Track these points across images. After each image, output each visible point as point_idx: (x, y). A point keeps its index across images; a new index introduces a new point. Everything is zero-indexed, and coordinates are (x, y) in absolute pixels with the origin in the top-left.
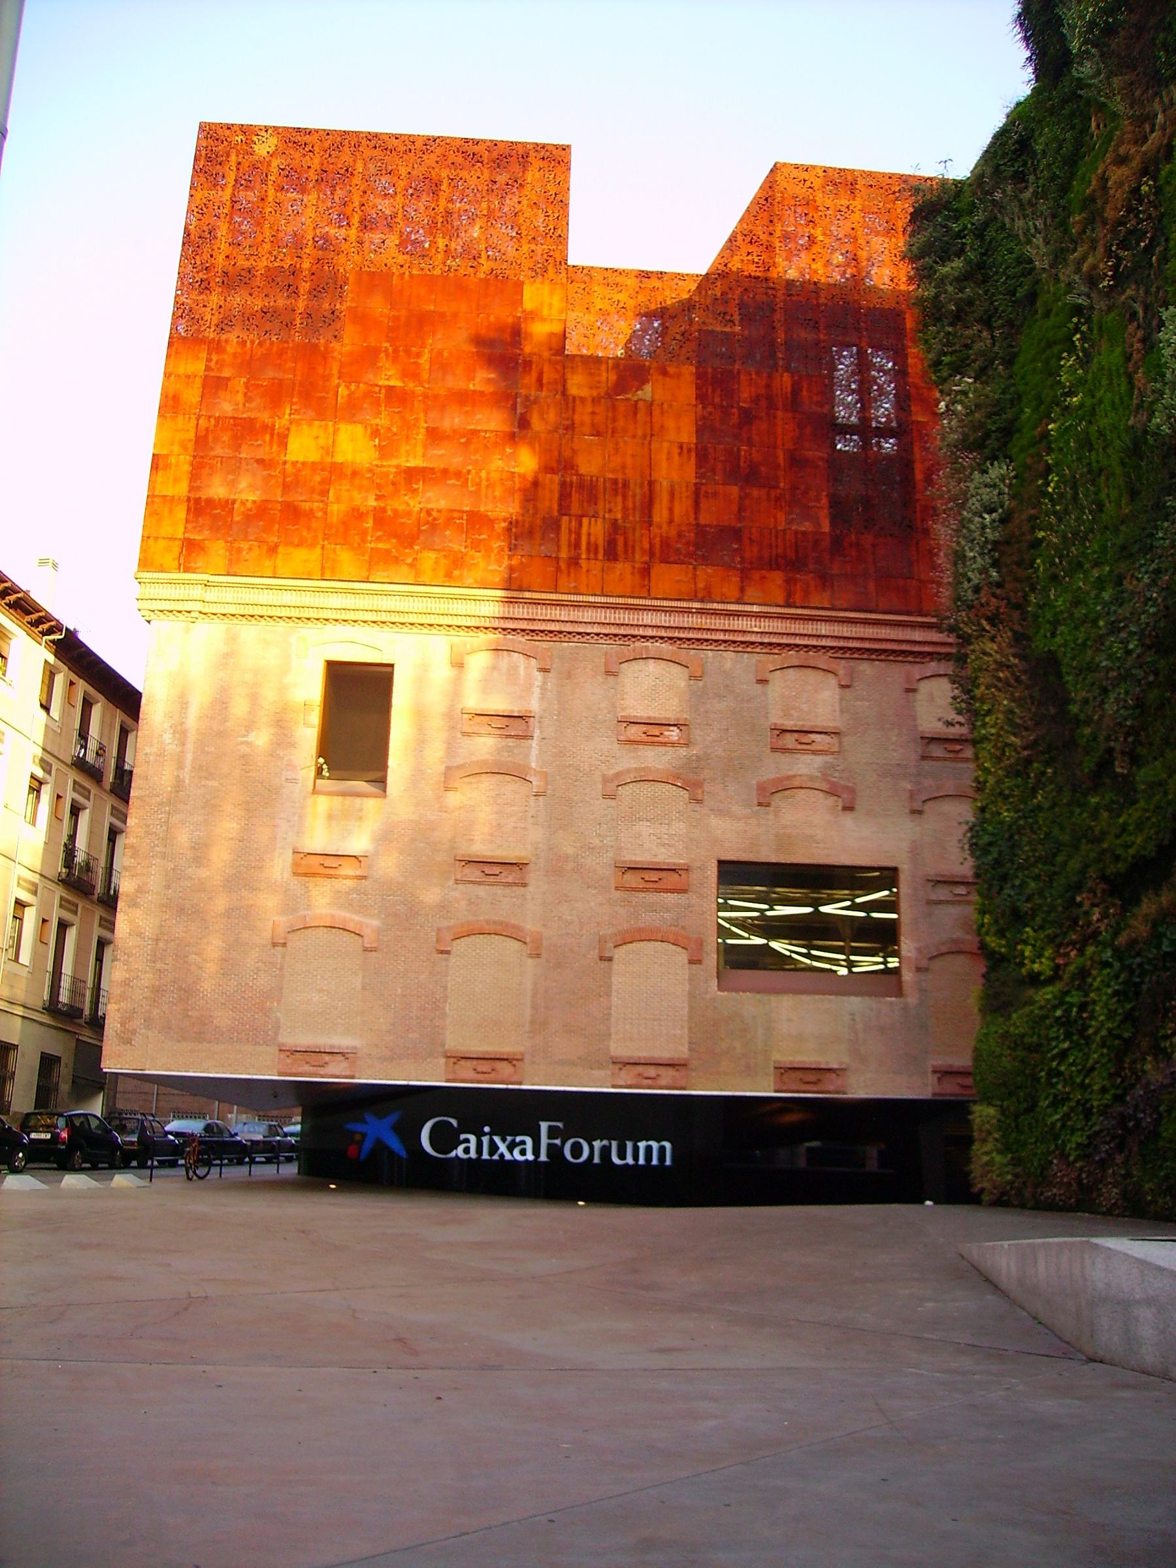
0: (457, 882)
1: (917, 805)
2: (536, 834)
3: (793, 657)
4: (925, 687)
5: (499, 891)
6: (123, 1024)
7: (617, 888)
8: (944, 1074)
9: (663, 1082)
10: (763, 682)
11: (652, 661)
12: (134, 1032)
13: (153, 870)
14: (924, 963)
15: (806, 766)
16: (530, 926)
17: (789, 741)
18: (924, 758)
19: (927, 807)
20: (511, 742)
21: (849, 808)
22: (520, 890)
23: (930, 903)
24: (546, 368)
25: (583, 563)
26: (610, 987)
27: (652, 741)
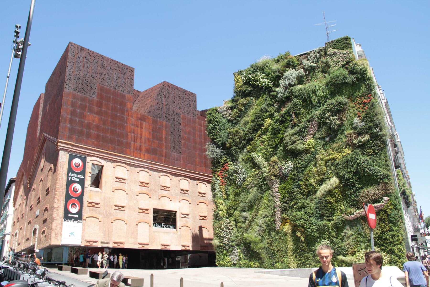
0: (114, 209)
1: (180, 201)
2: (126, 201)
3: (164, 174)
4: (181, 181)
5: (120, 211)
6: (55, 235)
7: (139, 212)
8: (184, 246)
9: (145, 247)
10: (160, 177)
11: (144, 172)
12: (58, 237)
13: (61, 203)
14: (181, 228)
15: (165, 193)
16: (126, 218)
17: (163, 188)
18: (181, 193)
19: (181, 201)
20: (123, 184)
21: (171, 201)
22: (124, 212)
23: (181, 217)
24: (130, 112)
25: (135, 152)
26: (137, 230)
27: (144, 186)
